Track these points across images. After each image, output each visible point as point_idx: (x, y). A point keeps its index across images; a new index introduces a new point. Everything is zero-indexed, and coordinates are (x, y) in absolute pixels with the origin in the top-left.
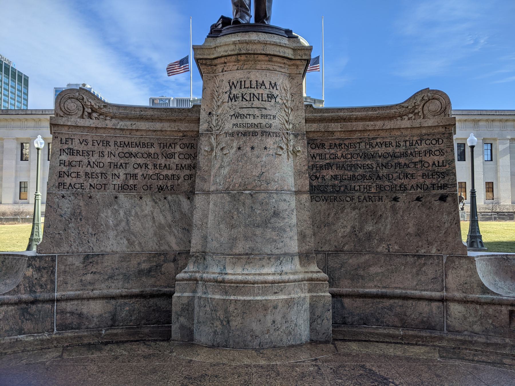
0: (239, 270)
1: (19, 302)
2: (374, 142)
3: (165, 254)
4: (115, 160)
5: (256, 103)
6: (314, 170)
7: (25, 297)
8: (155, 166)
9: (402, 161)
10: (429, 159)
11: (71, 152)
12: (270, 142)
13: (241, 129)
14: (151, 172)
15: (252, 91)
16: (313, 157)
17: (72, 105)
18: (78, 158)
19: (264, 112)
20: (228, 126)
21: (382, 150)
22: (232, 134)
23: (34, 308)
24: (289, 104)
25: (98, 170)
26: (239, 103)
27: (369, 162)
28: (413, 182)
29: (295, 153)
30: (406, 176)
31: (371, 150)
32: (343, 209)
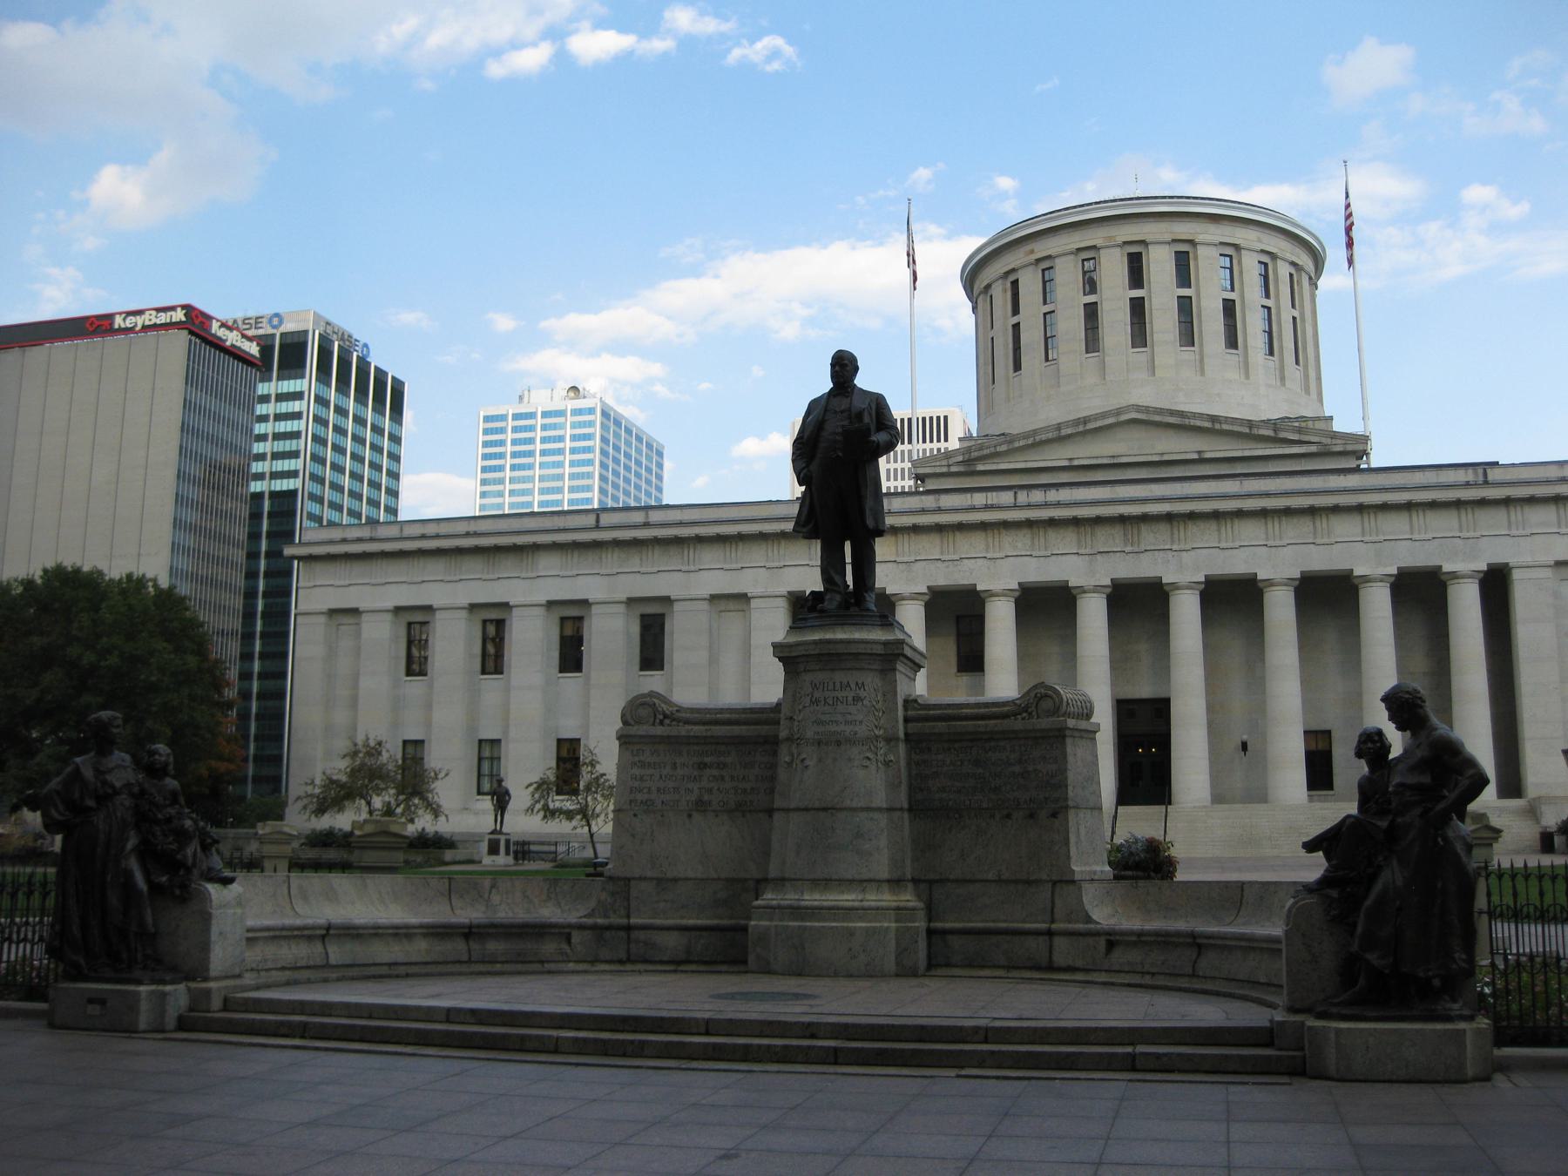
0: (817, 897)
1: (594, 927)
3: (746, 880)
5: (840, 708)
6: (917, 783)
7: (600, 921)
8: (732, 778)
11: (643, 765)
15: (837, 694)
16: (917, 764)
17: (643, 712)
19: (849, 717)
20: (809, 734)
23: (608, 934)
24: (879, 706)
25: (671, 784)
29: (887, 764)
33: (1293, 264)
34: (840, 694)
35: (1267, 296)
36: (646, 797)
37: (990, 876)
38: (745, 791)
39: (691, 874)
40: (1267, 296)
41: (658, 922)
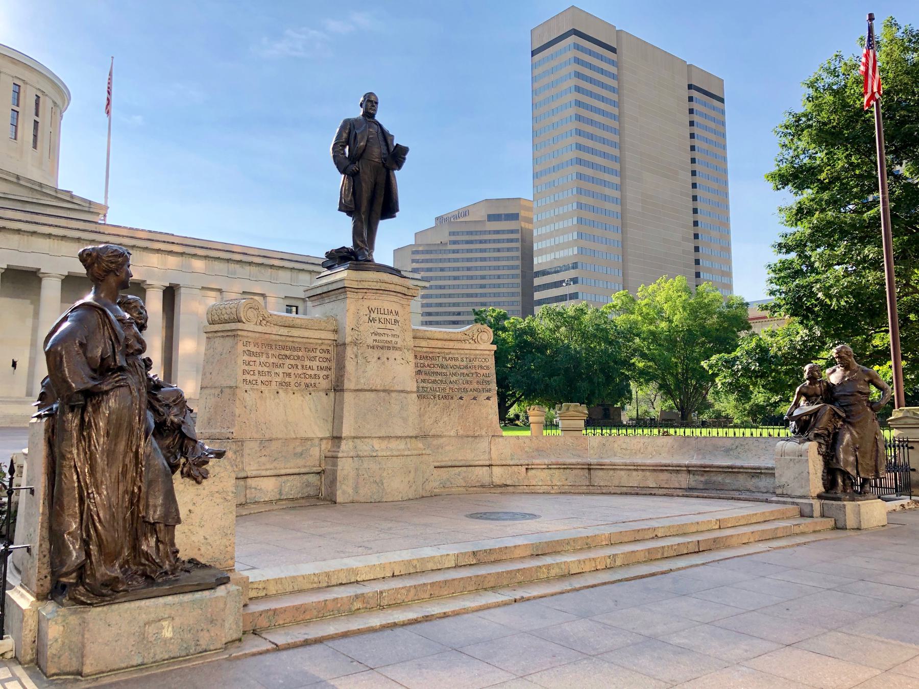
2: (448, 357)
3: (311, 439)
4: (272, 360)
8: (303, 366)
9: (465, 371)
10: (482, 372)
12: (397, 354)
13: (380, 344)
14: (300, 372)
18: (254, 359)
19: (394, 333)
20: (370, 341)
21: (453, 363)
22: (373, 347)
25: (266, 369)
26: (377, 324)
27: (444, 371)
28: (471, 387)
30: (467, 382)
31: (445, 363)
32: (429, 404)
33: (55, 103)
34: (388, 317)
35: (37, 115)
36: (252, 378)
37: (452, 433)
38: (310, 376)
39: (280, 436)
40: (37, 115)
41: (264, 473)
